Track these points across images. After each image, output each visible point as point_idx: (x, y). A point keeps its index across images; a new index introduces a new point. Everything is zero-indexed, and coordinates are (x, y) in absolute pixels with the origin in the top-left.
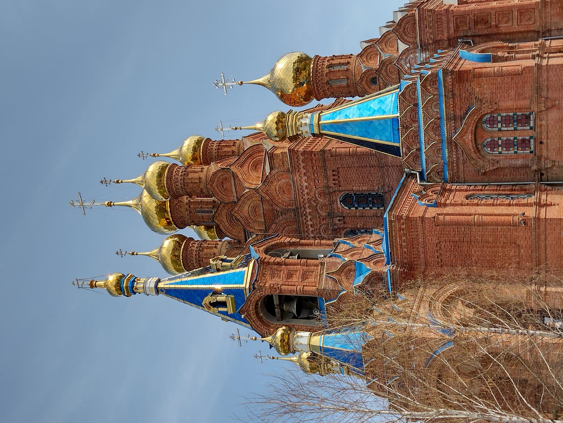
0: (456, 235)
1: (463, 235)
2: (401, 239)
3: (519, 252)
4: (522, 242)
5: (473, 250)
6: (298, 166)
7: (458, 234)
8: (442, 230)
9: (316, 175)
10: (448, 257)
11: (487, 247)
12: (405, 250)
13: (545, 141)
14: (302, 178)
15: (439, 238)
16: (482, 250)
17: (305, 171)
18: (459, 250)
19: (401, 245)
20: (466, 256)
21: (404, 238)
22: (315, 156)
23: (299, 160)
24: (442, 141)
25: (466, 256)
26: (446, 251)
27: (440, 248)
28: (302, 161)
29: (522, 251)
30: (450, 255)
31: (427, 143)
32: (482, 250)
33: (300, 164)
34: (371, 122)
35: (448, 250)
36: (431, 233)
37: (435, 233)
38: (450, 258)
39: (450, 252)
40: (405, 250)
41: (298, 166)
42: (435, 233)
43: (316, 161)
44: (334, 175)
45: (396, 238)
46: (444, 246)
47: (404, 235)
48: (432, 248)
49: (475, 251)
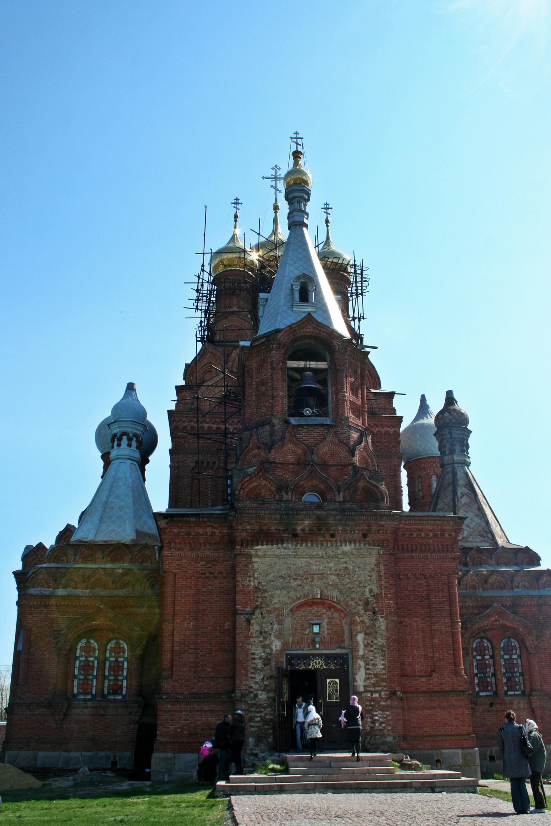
0: (438, 599)
1: (439, 608)
2: (430, 530)
3: (420, 676)
4: (436, 679)
5: (418, 619)
6: (381, 425)
7: (440, 601)
8: (442, 581)
10: (406, 588)
11: (424, 637)
12: (415, 535)
13: (493, 708)
15: (432, 577)
16: (419, 630)
17: (375, 432)
18: (417, 601)
19: (421, 530)
20: (409, 610)
21: (431, 534)
22: (393, 447)
23: (388, 427)
25: (409, 610)
26: (414, 586)
27: (418, 578)
28: (387, 431)
29: (424, 680)
30: (409, 590)
32: (419, 630)
33: (383, 428)
35: (415, 588)
36: (438, 569)
37: (439, 573)
38: (404, 590)
39: (413, 590)
40: (415, 535)
41: (381, 425)
42: (439, 573)
43: (387, 447)
45: (431, 525)
46: (421, 584)
47: (435, 536)
48: (418, 569)
49: (417, 621)
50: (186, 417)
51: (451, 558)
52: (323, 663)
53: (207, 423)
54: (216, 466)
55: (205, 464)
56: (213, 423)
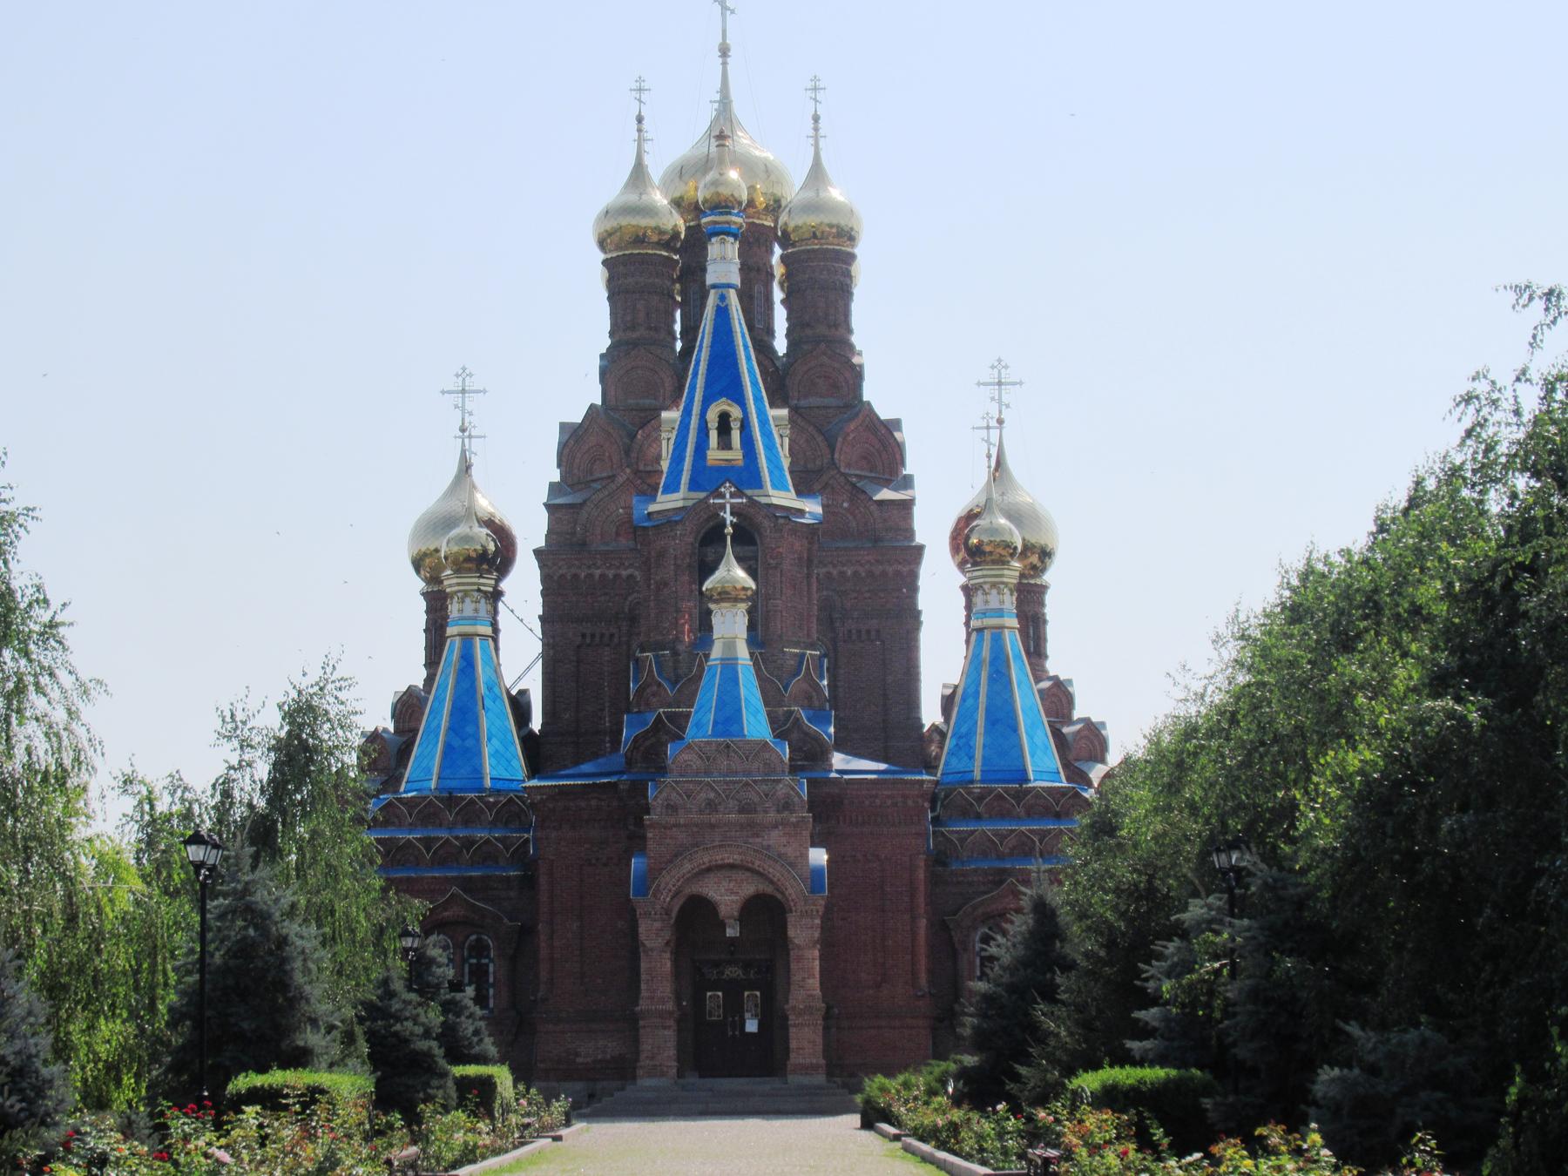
2: (888, 797)
9: (867, 595)
12: (867, 803)
14: (861, 565)
19: (876, 796)
21: (889, 802)
24: (1001, 857)
29: (871, 992)
31: (996, 833)
34: (1015, 729)
40: (867, 803)
44: (868, 632)
50: (563, 560)
51: (916, 834)
52: (740, 972)
53: (598, 568)
54: (616, 640)
55: (597, 639)
56: (608, 568)
